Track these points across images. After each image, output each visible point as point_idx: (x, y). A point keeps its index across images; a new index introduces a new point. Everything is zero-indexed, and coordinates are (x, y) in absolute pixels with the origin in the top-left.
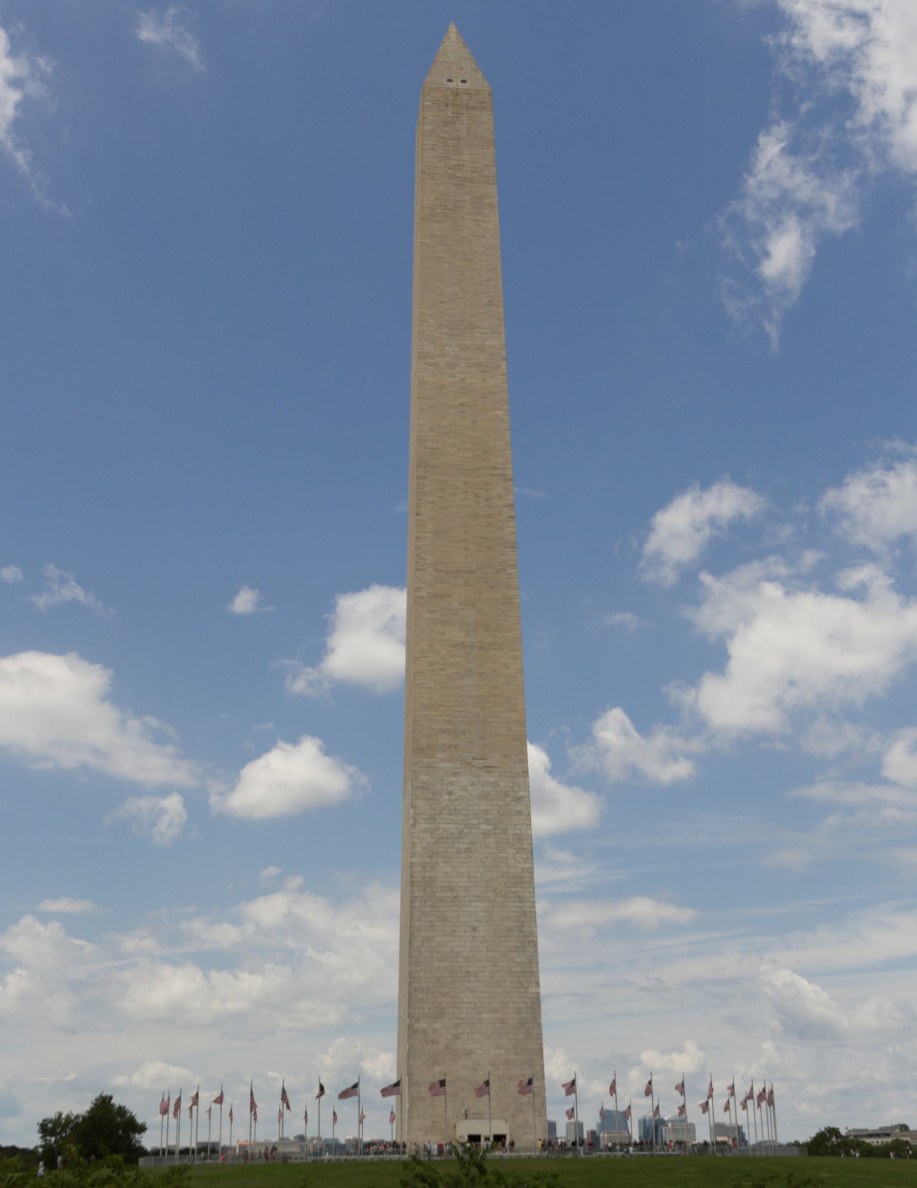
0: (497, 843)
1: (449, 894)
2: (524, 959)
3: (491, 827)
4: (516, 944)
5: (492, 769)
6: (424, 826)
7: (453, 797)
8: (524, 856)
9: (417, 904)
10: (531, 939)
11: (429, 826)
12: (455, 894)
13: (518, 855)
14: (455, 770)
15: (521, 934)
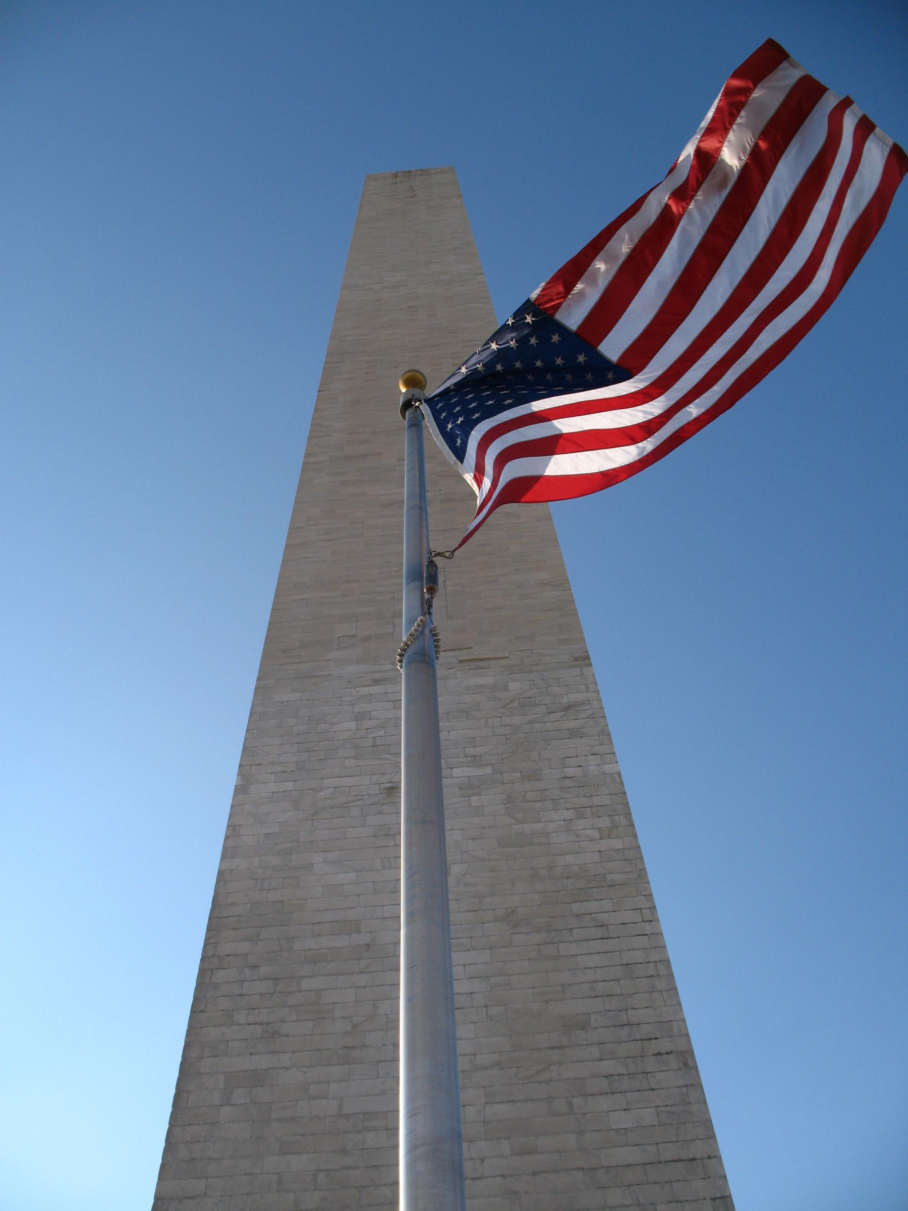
0: (509, 800)
1: (342, 941)
2: (648, 1116)
3: (489, 770)
4: (609, 1066)
5: (485, 663)
6: (272, 787)
7: (368, 723)
8: (605, 823)
9: (220, 976)
10: (664, 1045)
11: (289, 786)
12: (361, 939)
13: (582, 823)
14: (377, 676)
15: (624, 1033)
